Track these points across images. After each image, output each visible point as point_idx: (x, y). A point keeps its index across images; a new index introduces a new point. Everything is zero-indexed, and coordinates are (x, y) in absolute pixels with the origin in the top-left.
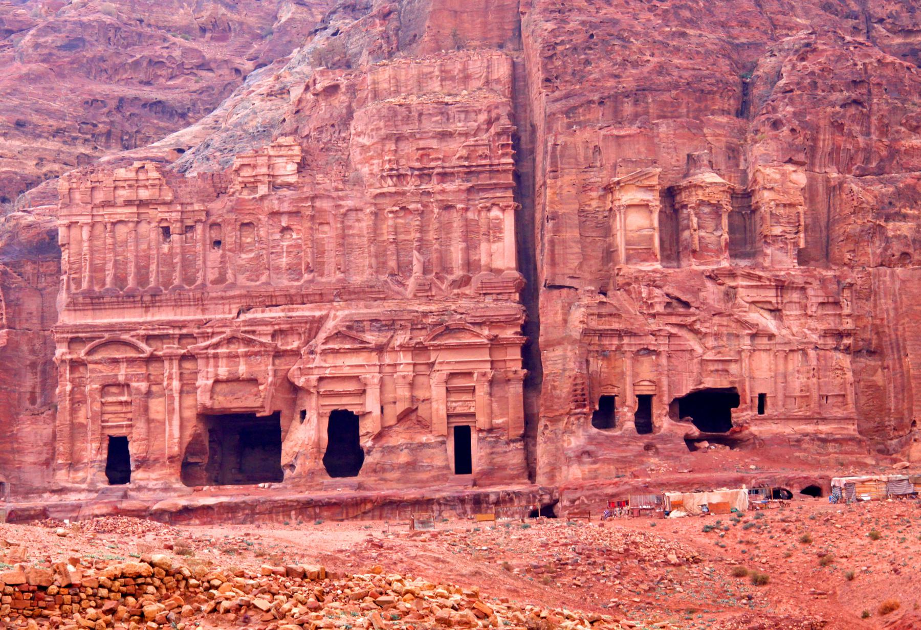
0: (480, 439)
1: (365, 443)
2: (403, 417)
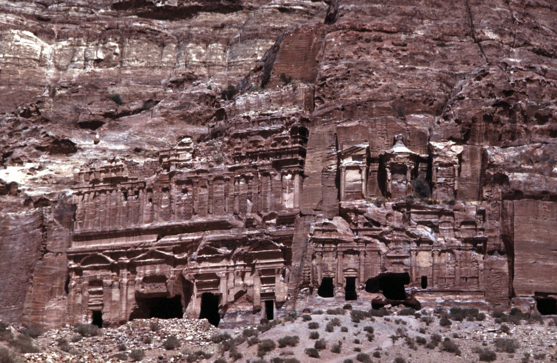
2: (238, 296)
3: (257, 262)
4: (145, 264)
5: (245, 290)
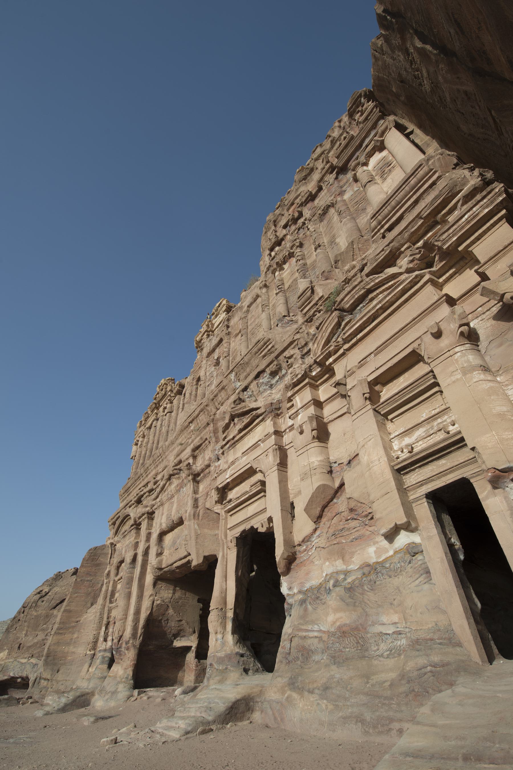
5: (337, 484)
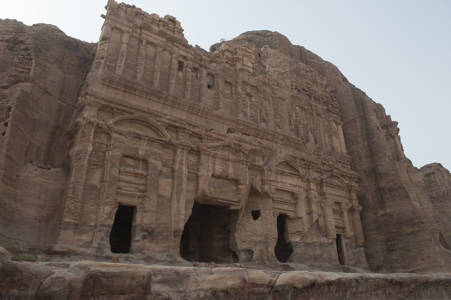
0: (346, 244)
1: (295, 239)
3: (328, 192)
4: (214, 156)
